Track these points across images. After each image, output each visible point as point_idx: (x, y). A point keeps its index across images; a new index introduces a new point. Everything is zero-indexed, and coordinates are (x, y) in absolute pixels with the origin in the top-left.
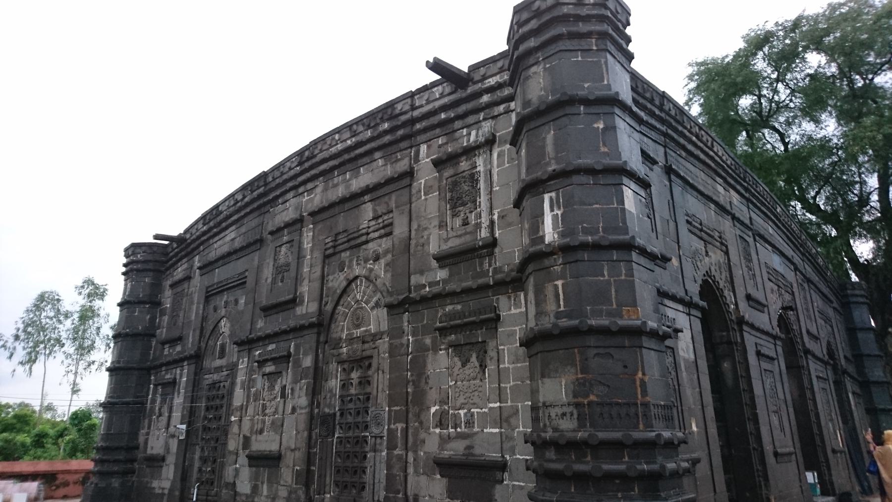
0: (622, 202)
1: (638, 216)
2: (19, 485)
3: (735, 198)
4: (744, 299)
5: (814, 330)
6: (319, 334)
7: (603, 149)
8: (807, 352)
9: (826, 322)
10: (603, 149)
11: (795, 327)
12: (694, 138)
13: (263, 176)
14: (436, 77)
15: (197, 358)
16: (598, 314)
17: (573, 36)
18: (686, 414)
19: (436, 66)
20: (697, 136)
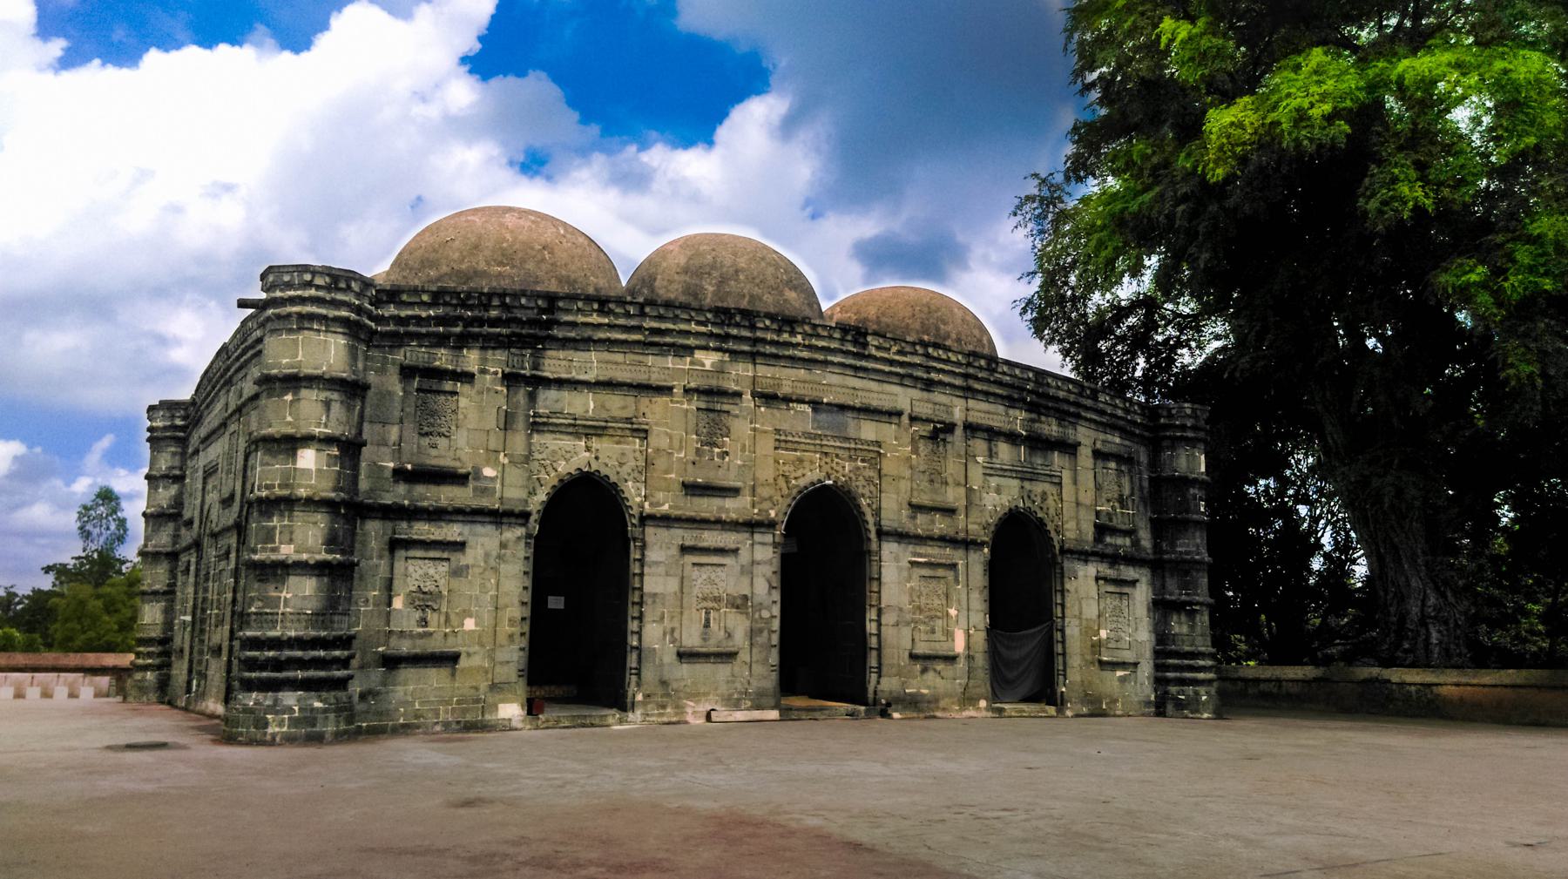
0: (294, 462)
1: (319, 471)
2: (88, 679)
3: (709, 359)
4: (678, 487)
5: (953, 496)
6: (239, 535)
7: (289, 419)
8: (881, 534)
9: (1022, 479)
10: (289, 419)
11: (863, 502)
12: (595, 319)
13: (224, 348)
14: (250, 311)
15: (197, 545)
16: (264, 550)
17: (279, 317)
18: (452, 617)
19: (243, 304)
20: (601, 312)
